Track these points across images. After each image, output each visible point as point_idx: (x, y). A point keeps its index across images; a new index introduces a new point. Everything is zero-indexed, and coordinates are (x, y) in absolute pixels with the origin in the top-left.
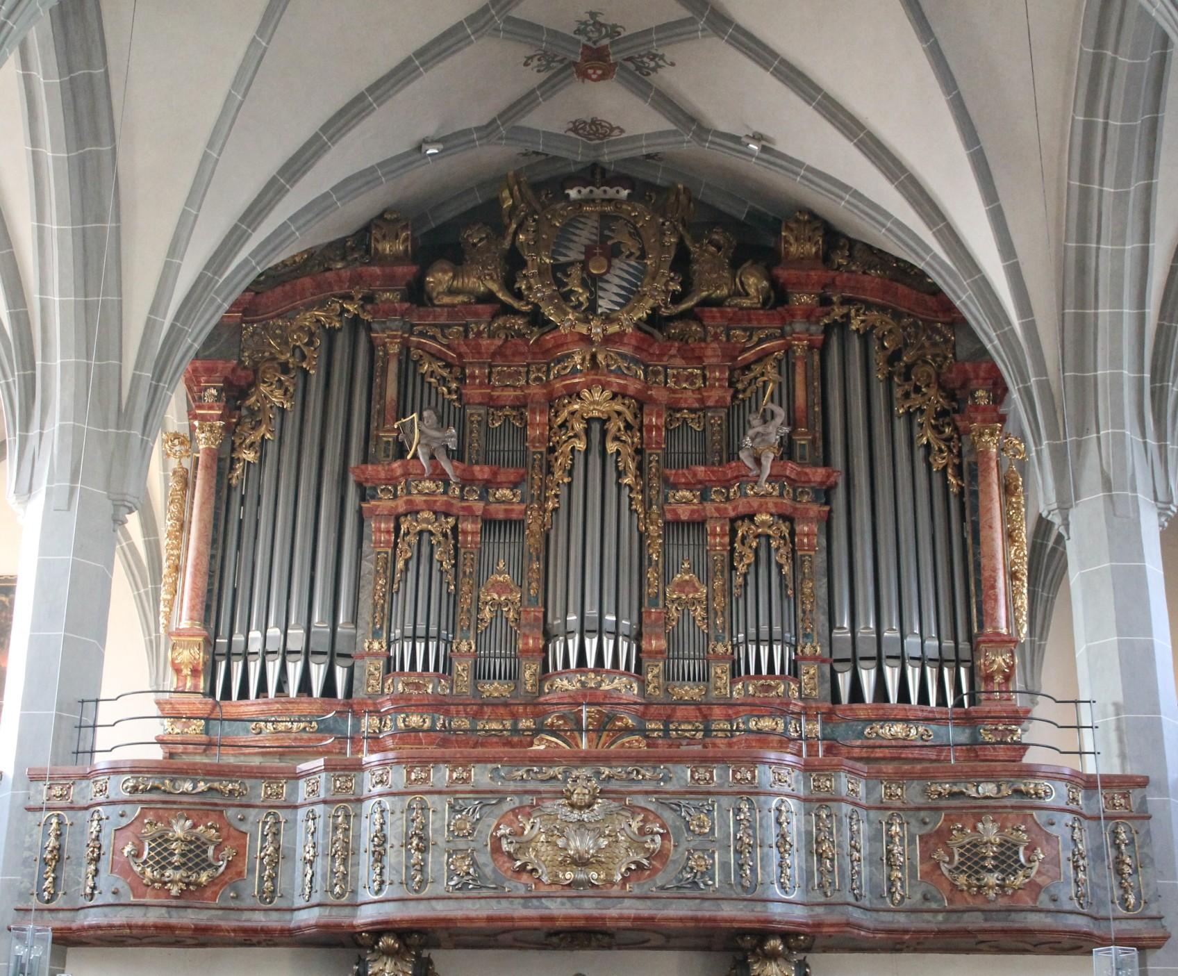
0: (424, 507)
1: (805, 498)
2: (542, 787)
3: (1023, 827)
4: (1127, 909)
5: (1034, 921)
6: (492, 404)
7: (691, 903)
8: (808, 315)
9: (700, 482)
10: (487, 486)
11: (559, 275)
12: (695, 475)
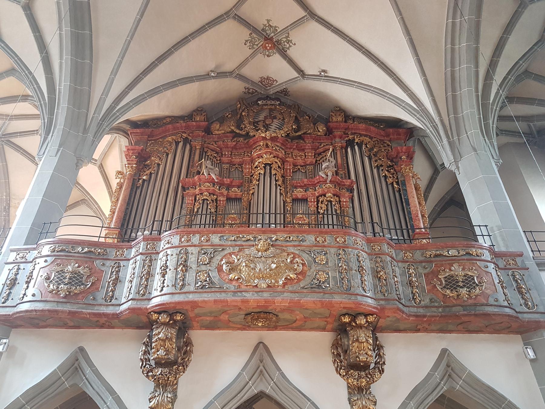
1: (344, 190)
2: (244, 243)
3: (474, 268)
4: (529, 308)
6: (231, 164)
7: (319, 295)
8: (341, 137)
10: (229, 187)
11: (255, 124)
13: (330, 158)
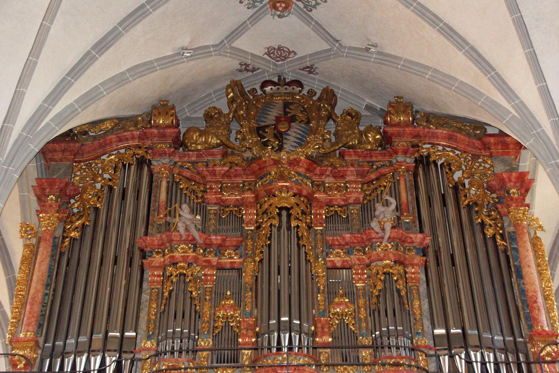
0: (181, 259)
9: (347, 244)
10: (220, 249)
11: (260, 132)
12: (344, 239)
13: (388, 197)
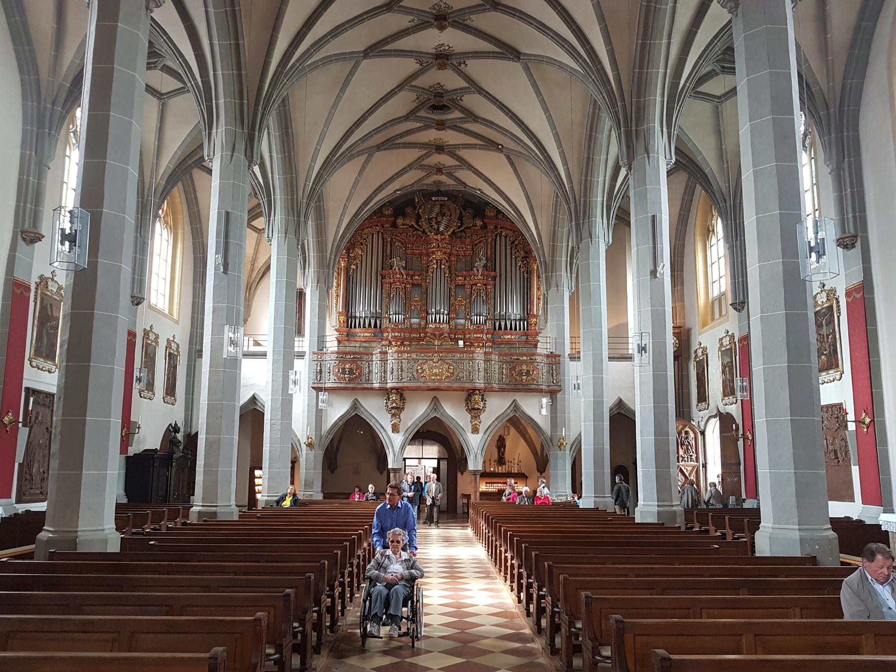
5: (533, 387)
6: (413, 254)
